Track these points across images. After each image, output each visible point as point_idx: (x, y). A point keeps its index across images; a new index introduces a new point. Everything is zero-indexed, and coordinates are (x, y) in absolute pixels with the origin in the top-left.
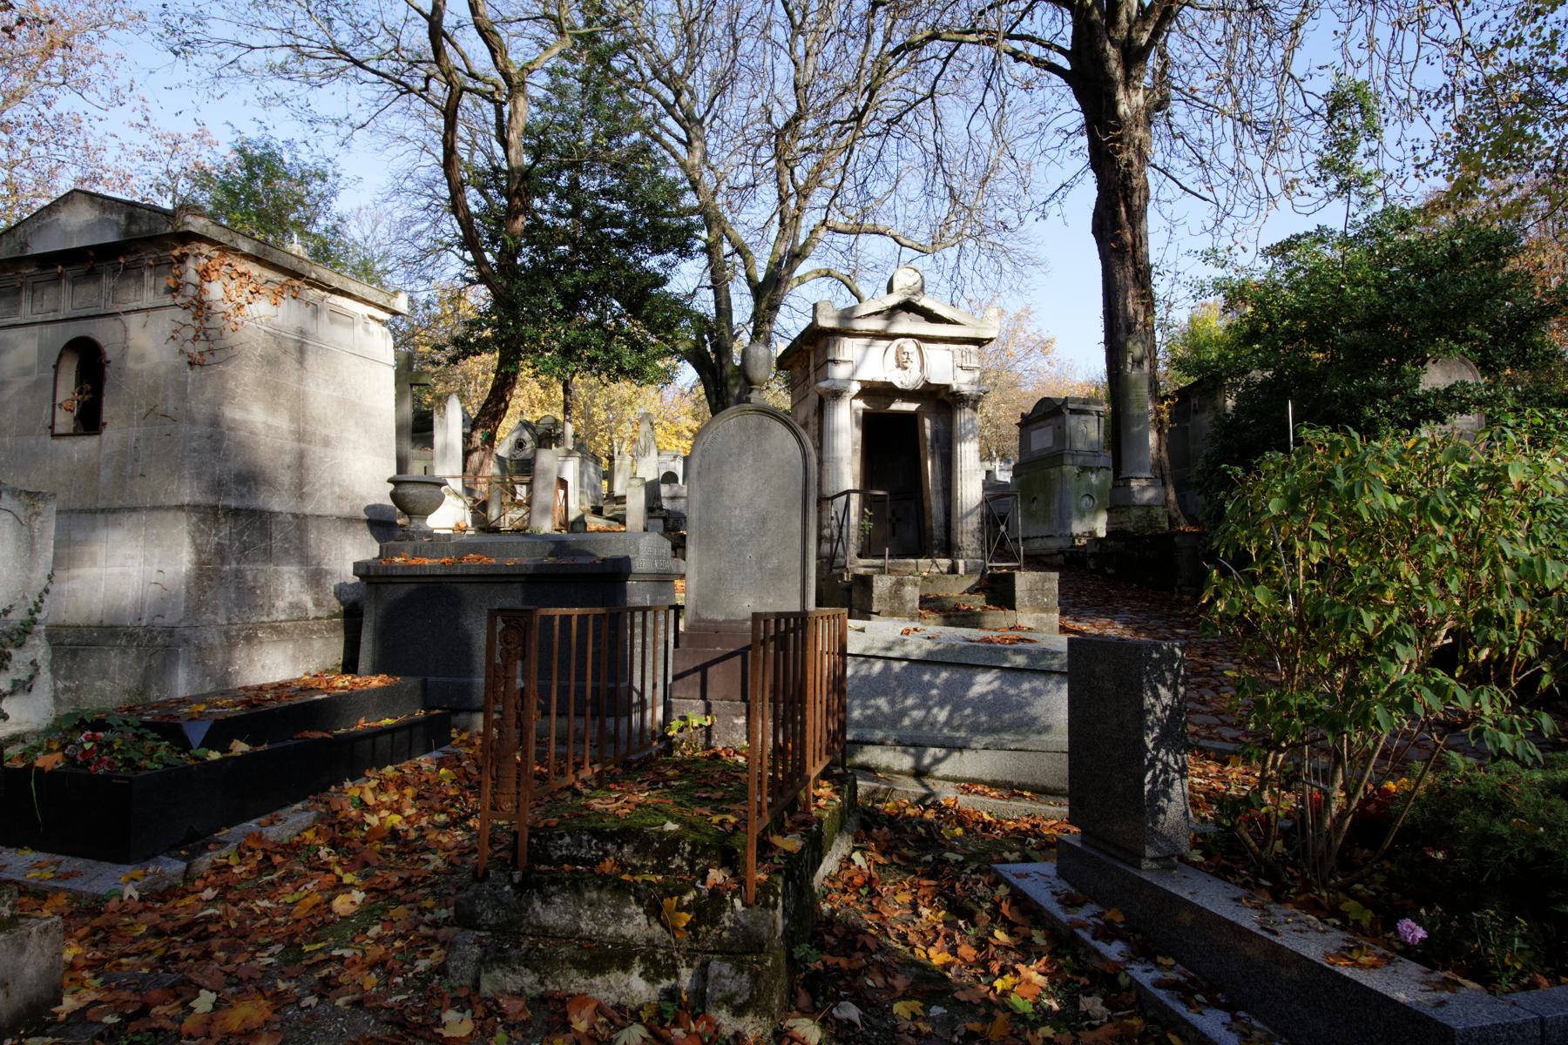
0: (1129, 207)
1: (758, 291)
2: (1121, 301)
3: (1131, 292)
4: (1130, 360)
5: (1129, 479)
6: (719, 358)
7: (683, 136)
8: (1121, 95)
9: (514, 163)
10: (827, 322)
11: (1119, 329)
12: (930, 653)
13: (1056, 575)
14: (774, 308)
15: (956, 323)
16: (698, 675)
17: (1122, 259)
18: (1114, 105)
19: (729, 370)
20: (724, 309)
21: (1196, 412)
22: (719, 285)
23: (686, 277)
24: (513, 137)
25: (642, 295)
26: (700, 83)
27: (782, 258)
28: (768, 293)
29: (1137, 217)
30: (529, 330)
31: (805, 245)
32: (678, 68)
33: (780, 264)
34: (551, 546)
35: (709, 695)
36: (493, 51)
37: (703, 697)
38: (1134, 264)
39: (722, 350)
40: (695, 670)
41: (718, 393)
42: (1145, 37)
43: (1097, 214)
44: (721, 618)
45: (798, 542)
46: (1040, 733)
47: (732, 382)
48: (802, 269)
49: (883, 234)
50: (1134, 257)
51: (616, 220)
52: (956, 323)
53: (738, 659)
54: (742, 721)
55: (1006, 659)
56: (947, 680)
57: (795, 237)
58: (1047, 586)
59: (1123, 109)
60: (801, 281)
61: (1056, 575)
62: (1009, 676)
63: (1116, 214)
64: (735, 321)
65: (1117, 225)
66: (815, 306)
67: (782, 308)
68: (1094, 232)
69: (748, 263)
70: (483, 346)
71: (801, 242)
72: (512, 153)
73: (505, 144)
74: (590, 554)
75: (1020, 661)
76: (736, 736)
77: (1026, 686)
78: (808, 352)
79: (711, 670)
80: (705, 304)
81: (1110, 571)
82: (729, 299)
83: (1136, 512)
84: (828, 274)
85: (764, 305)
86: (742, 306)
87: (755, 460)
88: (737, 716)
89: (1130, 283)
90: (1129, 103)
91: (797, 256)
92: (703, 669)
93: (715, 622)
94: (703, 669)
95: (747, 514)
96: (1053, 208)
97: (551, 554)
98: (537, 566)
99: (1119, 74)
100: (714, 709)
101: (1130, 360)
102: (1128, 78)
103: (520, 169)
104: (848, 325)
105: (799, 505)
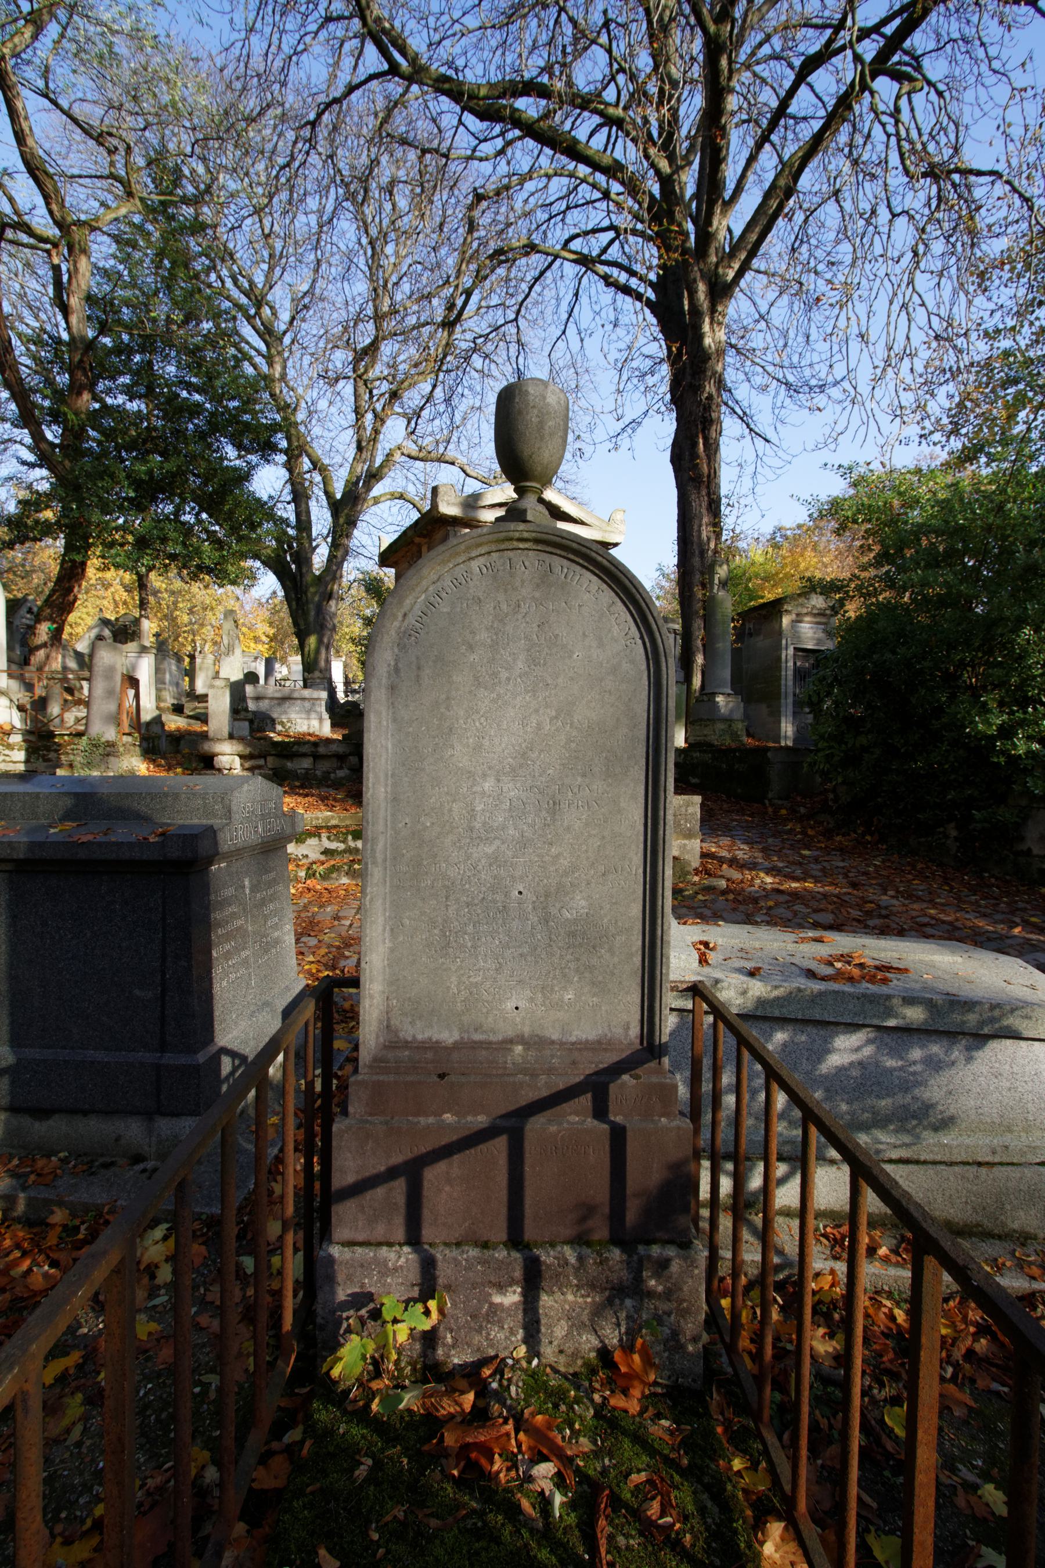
0: (706, 440)
1: (335, 507)
2: (696, 527)
3: (705, 520)
4: (716, 581)
5: (714, 694)
6: (299, 567)
7: (263, 347)
8: (706, 327)
9: (75, 330)
10: (449, 508)
11: (693, 554)
12: (761, 1002)
13: (698, 799)
14: (352, 523)
15: (582, 523)
16: (399, 1186)
17: (698, 489)
18: (700, 337)
19: (309, 579)
20: (304, 524)
21: (751, 635)
22: (300, 496)
23: (268, 481)
24: (75, 301)
25: (225, 494)
26: (281, 298)
27: (359, 479)
28: (347, 509)
29: (712, 449)
30: (96, 516)
31: (381, 466)
32: (259, 279)
33: (357, 483)
34: (69, 802)
35: (428, 1233)
36: (47, 198)
37: (413, 1240)
38: (709, 494)
39: (303, 558)
40: (392, 1173)
41: (298, 600)
42: (731, 274)
43: (675, 445)
44: (448, 1036)
45: (636, 857)
46: (936, 1129)
47: (312, 590)
48: (378, 490)
49: (453, 464)
50: (708, 487)
51: (196, 410)
52: (582, 523)
53: (500, 1145)
54: (512, 1297)
55: (889, 1013)
56: (785, 1045)
57: (372, 460)
58: (690, 810)
59: (708, 341)
60: (377, 501)
61: (698, 799)
62: (887, 1039)
63: (695, 444)
64: (314, 534)
65: (694, 455)
66: (435, 490)
67: (359, 524)
68: (672, 461)
69: (326, 481)
70: (47, 530)
72: (74, 319)
73: (65, 310)
74: (146, 819)
75: (915, 1015)
76: (497, 1334)
77: (916, 1054)
78: (419, 546)
79: (431, 1175)
80: (288, 512)
81: (694, 781)
83: (720, 726)
84: (401, 497)
85: (341, 520)
86: (321, 518)
88: (501, 1288)
89: (704, 511)
90: (712, 337)
91: (374, 476)
92: (412, 1172)
93: (434, 1046)
94: (412, 1172)
95: (512, 790)
96: (624, 441)
97: (67, 816)
98: (32, 845)
99: (705, 305)
100: (444, 1273)
101: (716, 581)
102: (713, 310)
103: (83, 338)
104: (472, 514)
105: (638, 772)
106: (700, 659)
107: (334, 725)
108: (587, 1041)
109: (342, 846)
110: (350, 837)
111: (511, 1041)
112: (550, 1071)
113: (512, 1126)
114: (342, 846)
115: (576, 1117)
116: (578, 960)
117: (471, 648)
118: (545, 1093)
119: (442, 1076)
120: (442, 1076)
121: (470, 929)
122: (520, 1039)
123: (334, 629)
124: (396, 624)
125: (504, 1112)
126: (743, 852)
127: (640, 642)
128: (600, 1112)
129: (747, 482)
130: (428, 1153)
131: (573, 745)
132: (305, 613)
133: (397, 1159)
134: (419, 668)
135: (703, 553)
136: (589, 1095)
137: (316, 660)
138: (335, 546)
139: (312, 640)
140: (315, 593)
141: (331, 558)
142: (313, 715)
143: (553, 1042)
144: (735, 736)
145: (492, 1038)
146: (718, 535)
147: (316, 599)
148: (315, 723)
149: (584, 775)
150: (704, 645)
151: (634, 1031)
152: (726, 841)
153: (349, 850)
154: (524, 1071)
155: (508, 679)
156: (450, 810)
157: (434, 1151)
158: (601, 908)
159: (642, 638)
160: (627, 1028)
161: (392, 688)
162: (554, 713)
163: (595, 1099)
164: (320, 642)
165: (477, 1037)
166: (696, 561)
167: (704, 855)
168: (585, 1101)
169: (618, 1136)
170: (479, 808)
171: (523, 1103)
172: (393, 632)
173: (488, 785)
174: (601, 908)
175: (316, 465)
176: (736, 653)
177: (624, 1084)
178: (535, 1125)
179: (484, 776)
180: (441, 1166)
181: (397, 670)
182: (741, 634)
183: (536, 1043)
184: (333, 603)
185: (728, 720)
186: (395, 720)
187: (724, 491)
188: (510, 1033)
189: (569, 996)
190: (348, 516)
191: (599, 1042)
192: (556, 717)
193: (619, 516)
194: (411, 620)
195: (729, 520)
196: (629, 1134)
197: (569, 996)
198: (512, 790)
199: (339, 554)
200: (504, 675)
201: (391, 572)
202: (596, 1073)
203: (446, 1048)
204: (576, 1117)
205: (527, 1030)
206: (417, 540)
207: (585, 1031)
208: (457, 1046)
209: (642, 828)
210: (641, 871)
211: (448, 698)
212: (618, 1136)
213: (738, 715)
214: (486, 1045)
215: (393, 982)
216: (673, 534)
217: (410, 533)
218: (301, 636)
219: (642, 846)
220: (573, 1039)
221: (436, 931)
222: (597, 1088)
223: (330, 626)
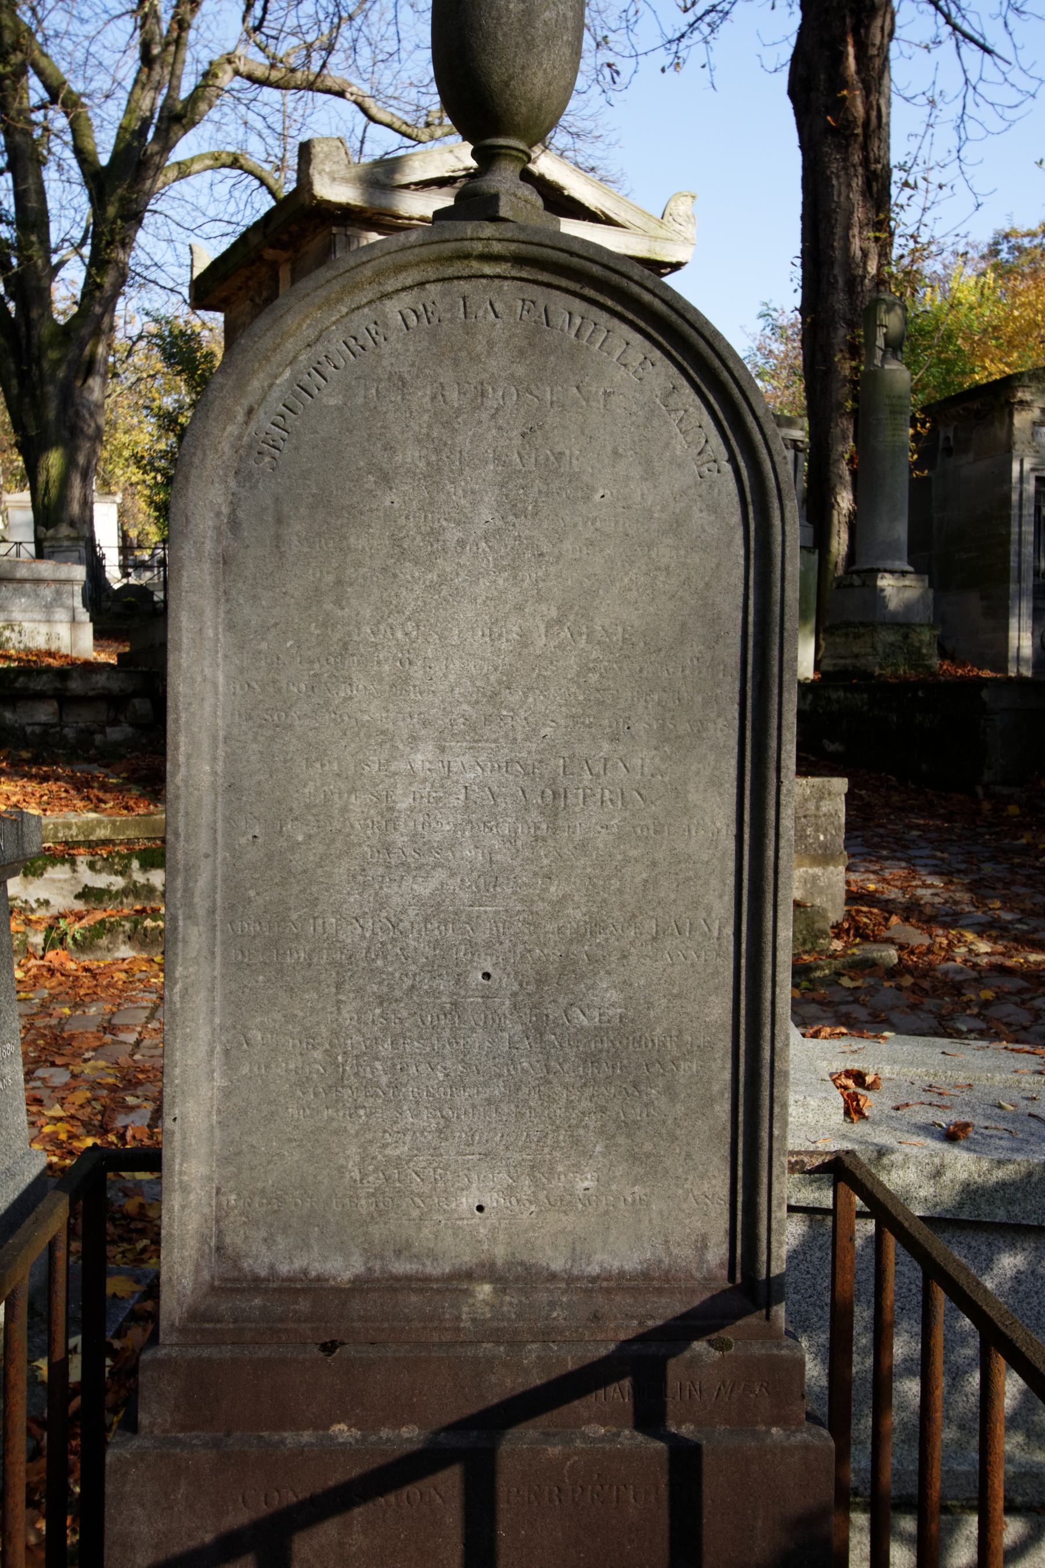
1: (98, 182)
2: (839, 231)
3: (859, 214)
4: (880, 342)
5: (874, 572)
10: (335, 189)
11: (833, 285)
12: (971, 1193)
13: (840, 785)
14: (134, 217)
15: (608, 221)
17: (844, 149)
19: (45, 332)
21: (949, 451)
27: (146, 123)
28: (122, 187)
31: (194, 98)
33: (142, 132)
38: (866, 162)
44: (342, 1267)
47: (53, 355)
48: (186, 147)
49: (341, 94)
50: (865, 148)
52: (608, 221)
53: (447, 1485)
56: (1018, 1278)
58: (826, 807)
60: (184, 171)
61: (840, 785)
63: (842, 56)
64: (54, 239)
65: (839, 81)
66: (305, 150)
68: (792, 93)
69: (78, 128)
71: (184, 94)
78: (274, 267)
81: (833, 747)
82: (41, 193)
83: (888, 637)
84: (235, 163)
85: (111, 211)
86: (68, 207)
87: (512, 508)
89: (856, 197)
91: (178, 118)
93: (311, 1288)
95: (469, 769)
96: (694, 50)
101: (880, 342)
104: (382, 201)
105: (724, 731)
106: (845, 501)
107: (100, 635)
108: (622, 1274)
109: (118, 882)
110: (135, 864)
111: (469, 1275)
112: (547, 1335)
113: (470, 1447)
114: (118, 882)
115: (601, 1427)
116: (603, 1110)
117: (386, 479)
118: (537, 1380)
119: (329, 1348)
120: (329, 1348)
121: (385, 1048)
122: (488, 1272)
123: (98, 436)
124: (232, 429)
125: (454, 1417)
126: (930, 889)
127: (727, 468)
128: (649, 1416)
129: (945, 137)
130: (301, 1505)
131: (593, 678)
132: (39, 405)
133: (238, 1518)
134: (279, 521)
135: (853, 283)
136: (627, 1383)
137: (63, 499)
138: (97, 264)
139: (54, 460)
140: (57, 364)
141: (91, 288)
142: (61, 614)
143: (553, 1277)
144: (915, 657)
145: (431, 1269)
146: (885, 247)
147: (61, 374)
148: (63, 630)
149: (614, 739)
150: (854, 473)
151: (717, 1253)
152: (895, 871)
153: (133, 890)
154: (496, 1336)
155: (462, 543)
156: (345, 810)
157: (313, 1500)
158: (650, 1006)
159: (732, 459)
160: (702, 1245)
161: (226, 561)
162: (554, 613)
163: (637, 1390)
164: (70, 463)
165: (402, 1267)
166: (839, 300)
167: (853, 897)
168: (619, 1394)
169: (685, 1463)
170: (403, 805)
171: (493, 1399)
172: (226, 447)
173: (422, 758)
174: (650, 1006)
175: (57, 92)
176: (918, 488)
177: (696, 1359)
178: (518, 1443)
179: (414, 739)
180: (329, 1530)
181: (234, 524)
182: (929, 450)
183: (519, 1278)
184: (95, 382)
185: (902, 624)
186: (231, 627)
187: (896, 155)
188: (467, 1259)
189: (586, 1182)
190: (124, 202)
191: (646, 1275)
192: (559, 621)
193: (683, 207)
194: (263, 420)
195: (906, 217)
196: (708, 1463)
197: (586, 1182)
198: (469, 769)
199: (108, 281)
200: (453, 534)
201: (216, 319)
202: (642, 1338)
203: (337, 1290)
204: (601, 1427)
205: (500, 1253)
206: (269, 254)
207: (620, 1254)
208: (360, 1286)
209: (731, 845)
210: (729, 930)
211: (339, 582)
212: (685, 1463)
213: (925, 615)
214: (419, 1283)
215: (229, 1157)
216: (794, 244)
217: (255, 240)
218: (31, 450)
219: (731, 881)
220: (594, 1269)
221: (318, 1055)
222: (642, 1366)
223: (91, 431)
